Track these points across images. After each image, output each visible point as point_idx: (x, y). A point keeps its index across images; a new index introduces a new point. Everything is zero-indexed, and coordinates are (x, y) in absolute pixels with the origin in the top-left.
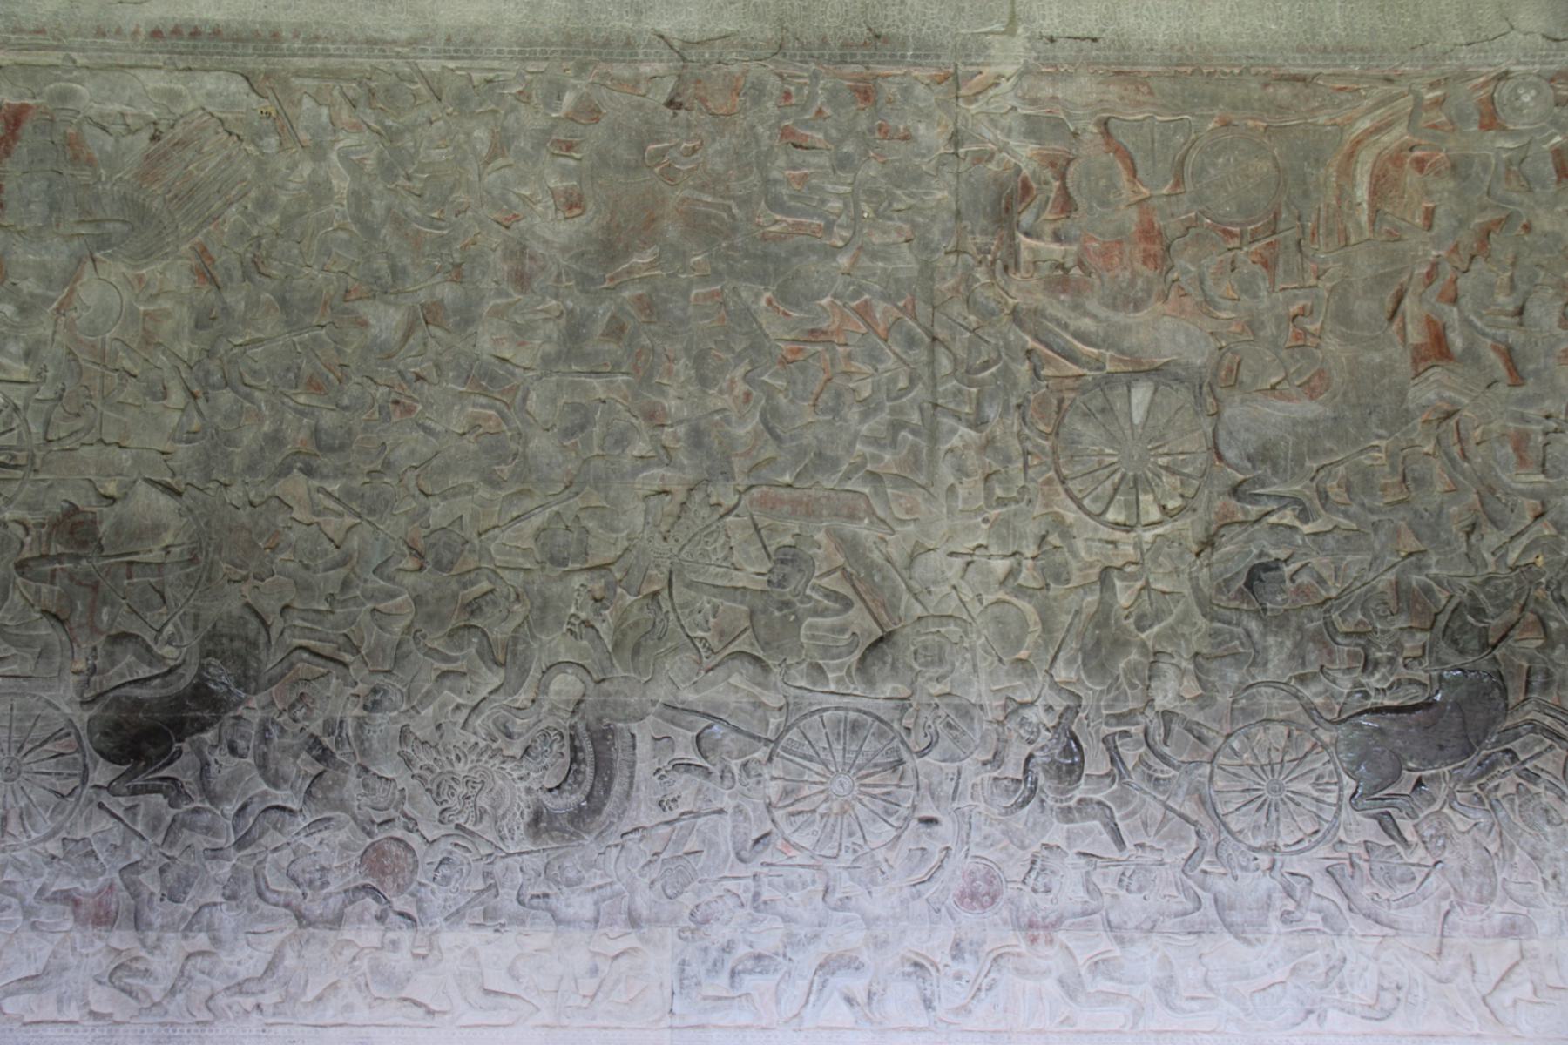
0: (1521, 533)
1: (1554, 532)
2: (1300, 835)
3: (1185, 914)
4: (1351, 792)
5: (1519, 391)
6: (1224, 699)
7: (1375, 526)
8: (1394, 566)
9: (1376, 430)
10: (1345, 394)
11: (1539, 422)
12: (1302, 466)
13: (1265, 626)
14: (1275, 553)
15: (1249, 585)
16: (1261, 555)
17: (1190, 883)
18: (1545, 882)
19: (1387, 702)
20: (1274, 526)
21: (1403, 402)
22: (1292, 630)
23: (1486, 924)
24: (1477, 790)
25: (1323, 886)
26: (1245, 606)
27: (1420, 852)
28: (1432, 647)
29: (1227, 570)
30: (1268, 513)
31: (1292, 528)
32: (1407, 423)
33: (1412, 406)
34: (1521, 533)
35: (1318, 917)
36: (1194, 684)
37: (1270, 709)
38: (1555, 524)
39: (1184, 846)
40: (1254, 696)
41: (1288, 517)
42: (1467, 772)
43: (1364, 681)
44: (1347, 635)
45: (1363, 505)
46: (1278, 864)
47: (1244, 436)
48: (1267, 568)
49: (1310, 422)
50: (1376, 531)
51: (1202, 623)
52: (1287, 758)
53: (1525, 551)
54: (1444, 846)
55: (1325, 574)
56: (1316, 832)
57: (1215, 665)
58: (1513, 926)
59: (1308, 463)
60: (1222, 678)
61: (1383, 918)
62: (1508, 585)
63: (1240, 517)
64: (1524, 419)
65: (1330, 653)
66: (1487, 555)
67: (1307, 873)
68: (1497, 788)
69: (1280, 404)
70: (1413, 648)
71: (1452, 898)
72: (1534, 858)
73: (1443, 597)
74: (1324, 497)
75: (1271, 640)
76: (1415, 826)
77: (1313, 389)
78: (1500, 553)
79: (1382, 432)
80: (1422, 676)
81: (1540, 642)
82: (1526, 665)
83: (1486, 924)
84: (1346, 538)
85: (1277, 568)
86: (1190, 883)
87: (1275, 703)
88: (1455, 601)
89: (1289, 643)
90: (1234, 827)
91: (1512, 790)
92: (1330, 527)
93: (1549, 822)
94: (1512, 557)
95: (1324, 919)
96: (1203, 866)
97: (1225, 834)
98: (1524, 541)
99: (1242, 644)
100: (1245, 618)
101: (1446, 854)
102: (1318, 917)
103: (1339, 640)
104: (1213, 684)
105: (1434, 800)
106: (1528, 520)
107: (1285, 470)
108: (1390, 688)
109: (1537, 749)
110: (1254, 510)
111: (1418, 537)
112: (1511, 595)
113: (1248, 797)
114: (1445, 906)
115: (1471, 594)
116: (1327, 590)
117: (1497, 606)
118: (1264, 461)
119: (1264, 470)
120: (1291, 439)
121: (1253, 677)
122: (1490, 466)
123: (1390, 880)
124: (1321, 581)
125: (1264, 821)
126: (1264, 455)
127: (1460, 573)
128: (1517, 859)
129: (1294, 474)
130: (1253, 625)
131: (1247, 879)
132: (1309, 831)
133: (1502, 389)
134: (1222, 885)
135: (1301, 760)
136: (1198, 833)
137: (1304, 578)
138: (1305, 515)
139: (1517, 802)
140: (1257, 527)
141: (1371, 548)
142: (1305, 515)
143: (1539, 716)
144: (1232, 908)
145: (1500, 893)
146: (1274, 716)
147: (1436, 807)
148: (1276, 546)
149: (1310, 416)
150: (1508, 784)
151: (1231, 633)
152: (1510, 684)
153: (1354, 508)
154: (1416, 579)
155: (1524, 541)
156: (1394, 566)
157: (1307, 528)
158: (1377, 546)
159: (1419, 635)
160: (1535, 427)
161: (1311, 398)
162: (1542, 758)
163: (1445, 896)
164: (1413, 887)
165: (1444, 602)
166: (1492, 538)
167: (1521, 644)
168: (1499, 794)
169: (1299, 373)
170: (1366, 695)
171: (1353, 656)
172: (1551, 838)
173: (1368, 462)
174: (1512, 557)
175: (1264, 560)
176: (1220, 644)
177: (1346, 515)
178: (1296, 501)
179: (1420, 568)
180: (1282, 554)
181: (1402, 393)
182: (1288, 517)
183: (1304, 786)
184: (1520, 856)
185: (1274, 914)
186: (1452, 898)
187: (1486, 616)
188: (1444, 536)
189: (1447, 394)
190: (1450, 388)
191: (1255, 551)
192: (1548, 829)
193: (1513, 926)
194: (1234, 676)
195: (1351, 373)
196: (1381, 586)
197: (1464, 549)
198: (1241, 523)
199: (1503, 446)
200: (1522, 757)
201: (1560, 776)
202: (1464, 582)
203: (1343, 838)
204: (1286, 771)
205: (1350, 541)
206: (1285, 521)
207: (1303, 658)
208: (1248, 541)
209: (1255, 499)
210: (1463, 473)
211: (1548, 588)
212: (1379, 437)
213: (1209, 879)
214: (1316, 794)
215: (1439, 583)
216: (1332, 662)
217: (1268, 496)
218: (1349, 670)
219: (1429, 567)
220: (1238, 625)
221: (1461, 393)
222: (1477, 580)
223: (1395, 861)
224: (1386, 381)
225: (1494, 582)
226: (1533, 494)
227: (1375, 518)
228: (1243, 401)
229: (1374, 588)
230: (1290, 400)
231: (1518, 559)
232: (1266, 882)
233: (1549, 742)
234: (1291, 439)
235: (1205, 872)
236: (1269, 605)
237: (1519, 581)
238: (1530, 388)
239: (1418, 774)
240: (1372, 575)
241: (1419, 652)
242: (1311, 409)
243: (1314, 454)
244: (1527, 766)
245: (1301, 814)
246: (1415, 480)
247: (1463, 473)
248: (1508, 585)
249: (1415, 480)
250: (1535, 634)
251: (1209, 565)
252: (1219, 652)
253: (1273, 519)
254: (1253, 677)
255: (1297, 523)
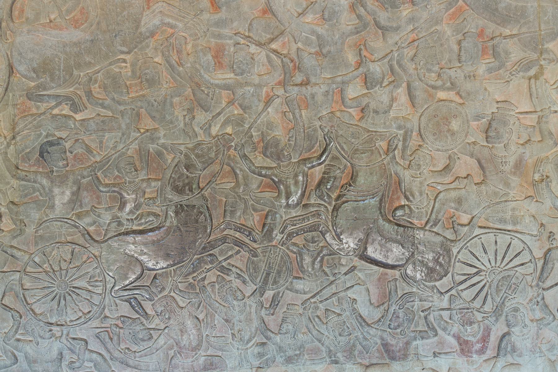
0: (219, 114)
1: (241, 112)
2: (81, 314)
3: (6, 367)
4: (112, 285)
5: (217, 17)
6: (30, 230)
7: (122, 113)
8: (136, 139)
9: (119, 48)
10: (98, 24)
11: (231, 38)
12: (71, 74)
13: (52, 182)
14: (58, 134)
15: (41, 155)
16: (47, 136)
17: (8, 347)
18: (233, 334)
19: (135, 228)
20: (54, 116)
21: (137, 27)
22: (70, 184)
23: (195, 364)
24: (192, 281)
25: (94, 345)
26: (41, 170)
27: (157, 321)
28: (161, 190)
29: (26, 147)
30: (52, 108)
31: (69, 117)
32: (141, 42)
33: (143, 30)
34: (219, 114)
35: (92, 364)
36: (10, 222)
37: (60, 235)
38: (241, 106)
39: (5, 324)
40: (48, 227)
41: (66, 110)
42: (184, 270)
43: (119, 215)
44: (107, 185)
45: (113, 99)
46: (65, 332)
47: (30, 55)
48: (51, 144)
49: (75, 44)
50: (122, 116)
51: (14, 183)
52: (71, 266)
53: (224, 125)
54: (169, 318)
55: (93, 145)
56: (90, 312)
57: (22, 208)
58: (211, 364)
59: (75, 72)
60: (28, 216)
61: (131, 362)
62: (209, 149)
63: (34, 111)
64: (219, 36)
65: (98, 197)
66: (197, 129)
67: (85, 338)
68: (204, 279)
69: (54, 32)
70: (152, 192)
71: (175, 348)
72: (227, 321)
73: (169, 158)
74: (89, 94)
75: (56, 190)
76: (153, 305)
77: (77, 21)
78: (207, 128)
79: (125, 49)
80: (157, 210)
81: (233, 184)
82: (224, 200)
83: (195, 364)
84: (102, 121)
85: (59, 144)
86: (8, 347)
87: (63, 231)
88: (176, 160)
89: (68, 193)
90: (37, 311)
91: (214, 279)
92: (94, 115)
93: (236, 299)
94: (215, 130)
95: (95, 365)
96: (18, 337)
97: (30, 317)
98: (222, 118)
99: (41, 194)
100: (39, 177)
101: (171, 322)
102: (92, 364)
103: (101, 189)
104: (22, 221)
105: (163, 289)
106: (224, 104)
107: (59, 78)
108: (136, 219)
109: (230, 253)
110: (43, 106)
111: (153, 118)
112: (213, 155)
113: (47, 291)
114: (171, 353)
115: (186, 155)
116: (94, 157)
117: (203, 163)
118: (44, 72)
119: (45, 79)
120: (62, 56)
121: (47, 215)
122: (197, 70)
123: (136, 340)
124: (89, 150)
125: (57, 307)
126: (44, 68)
127: (181, 142)
128: (216, 322)
129: (65, 81)
130: (45, 182)
131: (44, 343)
132: (86, 311)
133: (206, 16)
134: (29, 349)
135: (78, 267)
136: (12, 316)
137: (79, 150)
138: (75, 108)
139: (217, 287)
140: (42, 117)
141: (120, 128)
142: (75, 108)
143: (232, 232)
144: (35, 362)
145: (204, 344)
146: (63, 239)
147: (165, 293)
148: (58, 129)
149: (75, 40)
150: (212, 276)
151: (33, 188)
152: (214, 212)
153: (108, 102)
154: (152, 147)
155: (222, 118)
156: (136, 139)
157: (78, 117)
158: (124, 126)
159: (153, 184)
160: (228, 41)
161: (75, 27)
162: (234, 258)
163: (171, 348)
164: (150, 343)
165: (169, 161)
166: (201, 117)
167: (221, 186)
168: (206, 282)
169: (69, 12)
170: (120, 224)
171: (113, 199)
172: (237, 308)
173: (117, 70)
174: (215, 130)
175: (50, 139)
176: (26, 195)
177: (103, 106)
178: (68, 98)
179: (153, 140)
180: (63, 134)
181: (137, 23)
182: (66, 110)
183: (82, 283)
184: (218, 320)
185: (64, 363)
186: (175, 348)
187: (196, 169)
188: (168, 117)
189: (167, 20)
190: (168, 16)
191: (44, 133)
192: (235, 303)
193: (211, 364)
194: (36, 215)
195: (102, 9)
196: (130, 153)
197: (182, 125)
198: (32, 115)
199: (205, 55)
200: (220, 259)
201: (244, 270)
202: (182, 148)
203: (108, 314)
204: (69, 275)
205: (104, 125)
206: (64, 112)
207: (81, 201)
208: (38, 127)
209: (40, 98)
210: (179, 75)
211: (235, 149)
212: (122, 52)
213: (20, 344)
214: (90, 288)
215: (166, 149)
216: (99, 203)
217: (48, 95)
218: (110, 208)
219: (159, 138)
220: (35, 182)
221: (177, 19)
222: (190, 146)
223: (138, 328)
224: (125, 13)
225: (200, 147)
226: (226, 87)
227: (122, 108)
228: (29, 32)
229: (124, 154)
230: (61, 29)
231: (218, 131)
232: (56, 346)
233: (238, 248)
234: (62, 56)
235: (18, 340)
236: (55, 169)
237: (217, 146)
238: (223, 14)
239: (155, 272)
240: (122, 146)
241: (154, 195)
242: (77, 35)
243: (79, 66)
244: (224, 264)
245: (81, 301)
246: (147, 80)
247: (179, 75)
248: (209, 149)
249: (147, 80)
250: (230, 179)
251: (15, 144)
252: (26, 200)
253: (56, 111)
254: (47, 215)
255: (72, 114)
